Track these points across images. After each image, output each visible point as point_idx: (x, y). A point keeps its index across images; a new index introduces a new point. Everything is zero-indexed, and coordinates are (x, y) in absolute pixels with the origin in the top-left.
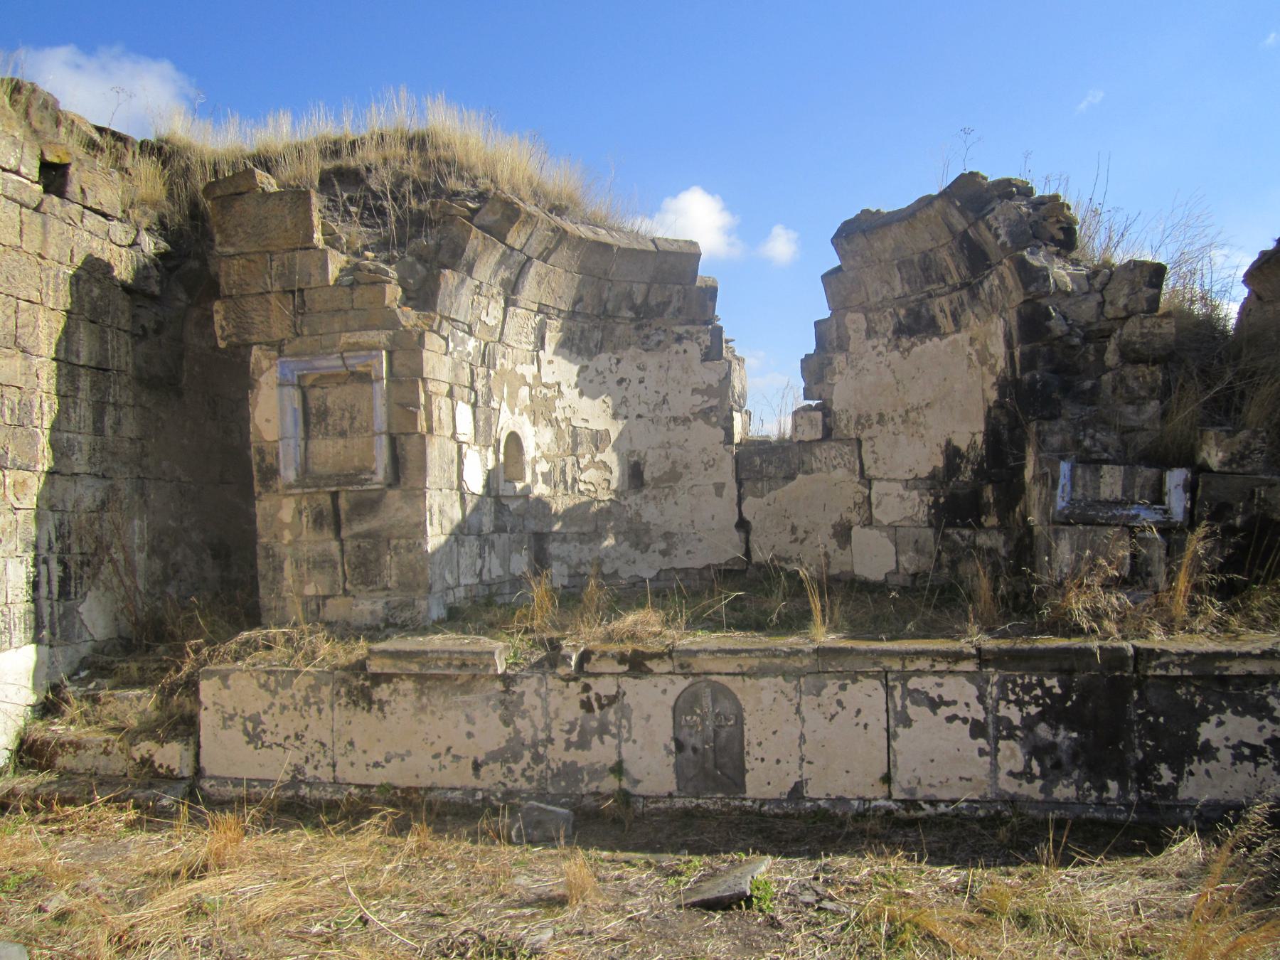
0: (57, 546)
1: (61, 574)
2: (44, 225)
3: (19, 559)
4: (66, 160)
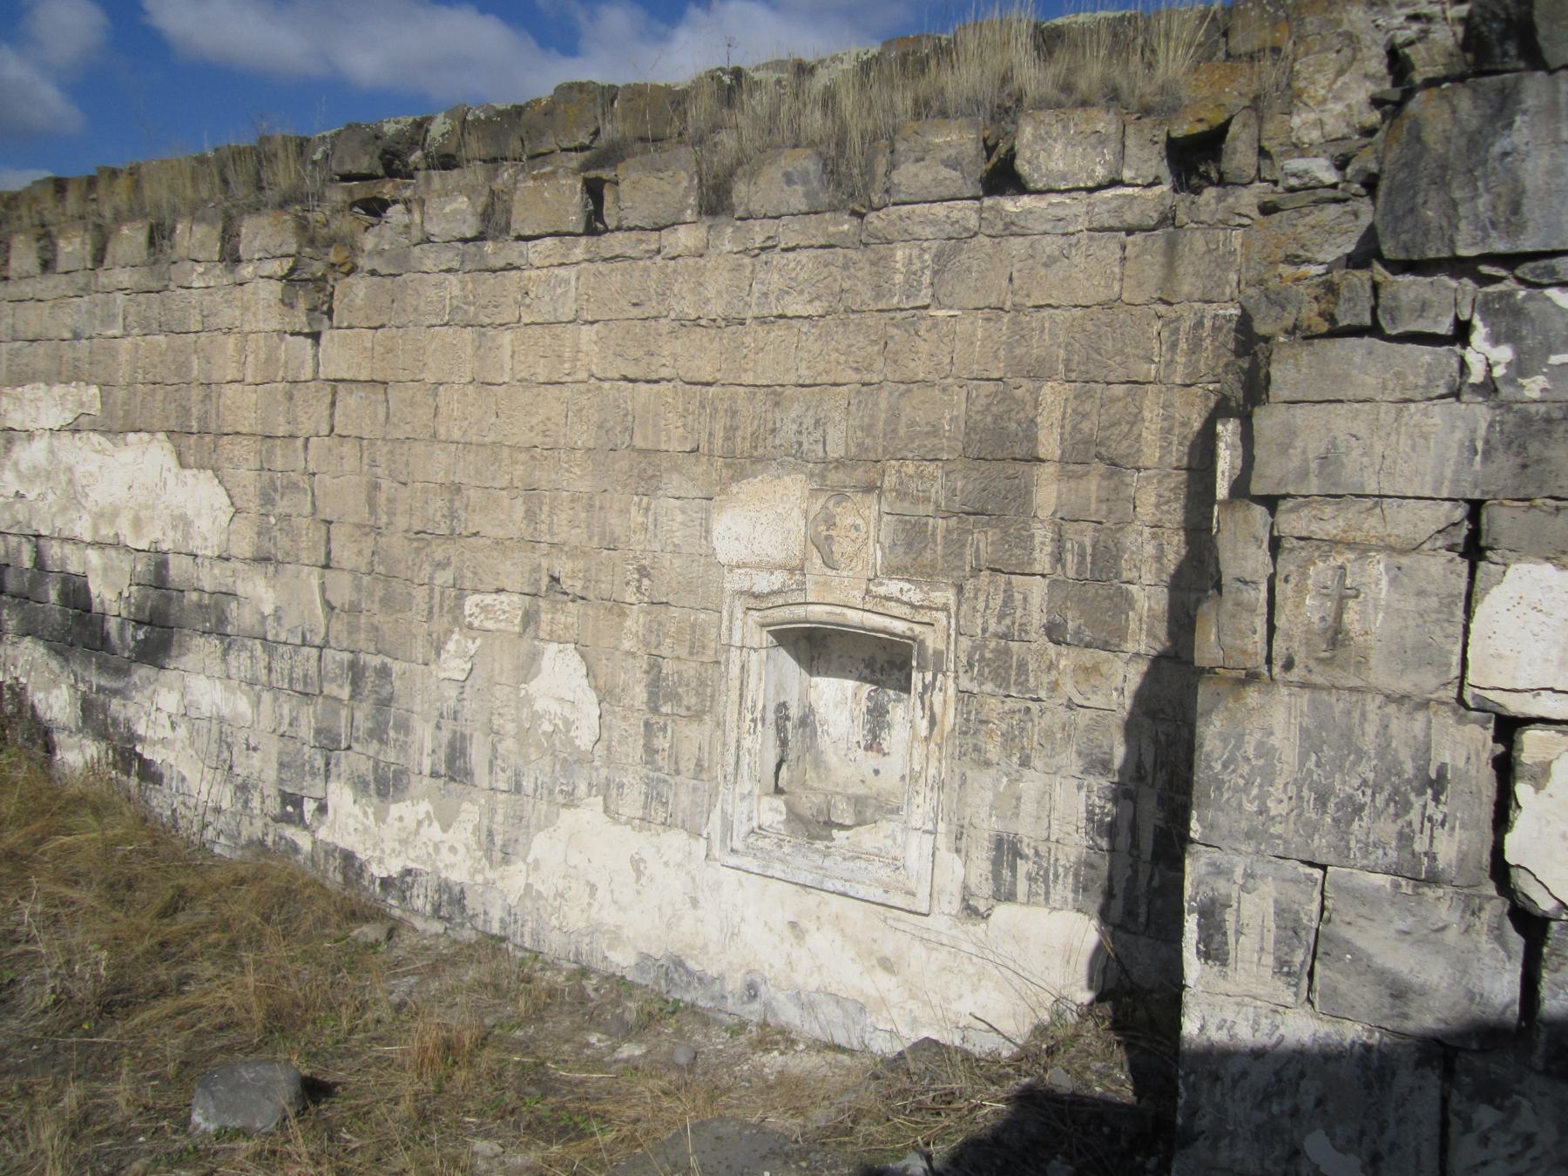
1: (1160, 823)
2: (1171, 248)
3: (1076, 782)
4: (1220, 119)
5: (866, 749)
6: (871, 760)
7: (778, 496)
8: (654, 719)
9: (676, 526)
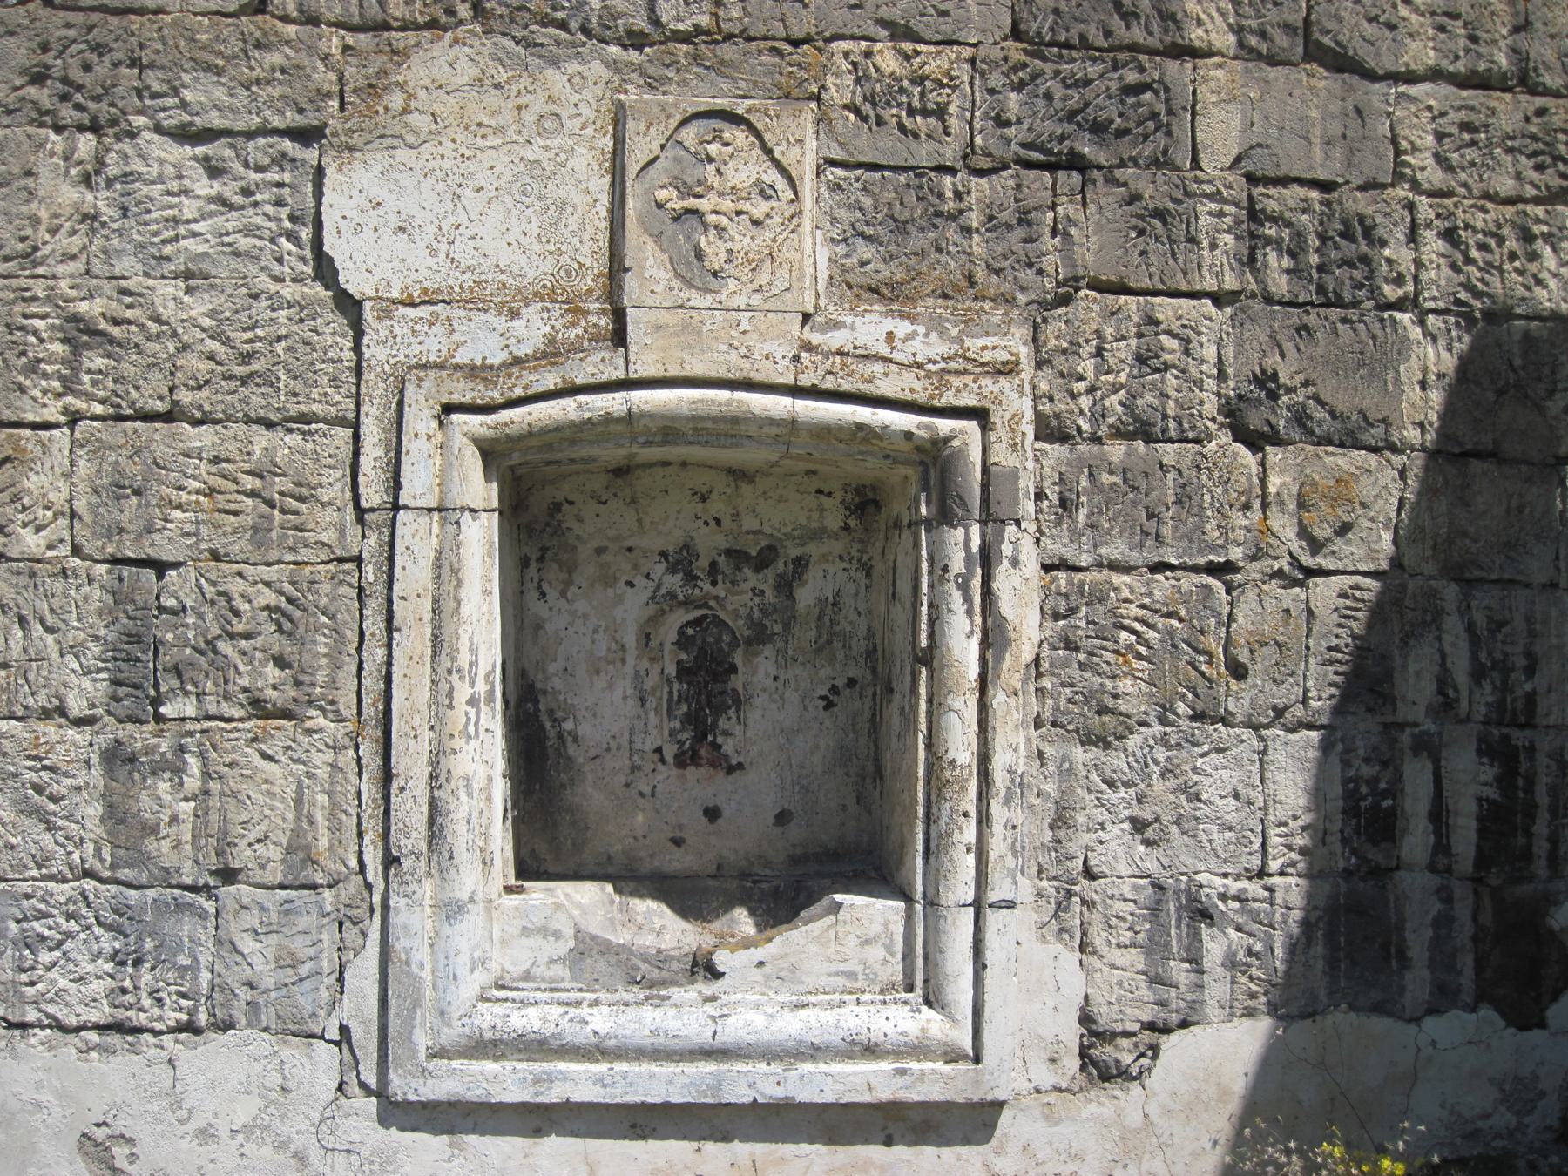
0: (1478, 701)
1: (1492, 793)
5: (681, 761)
6: (701, 785)
7: (529, 117)
8: (139, 737)
9: (189, 208)
